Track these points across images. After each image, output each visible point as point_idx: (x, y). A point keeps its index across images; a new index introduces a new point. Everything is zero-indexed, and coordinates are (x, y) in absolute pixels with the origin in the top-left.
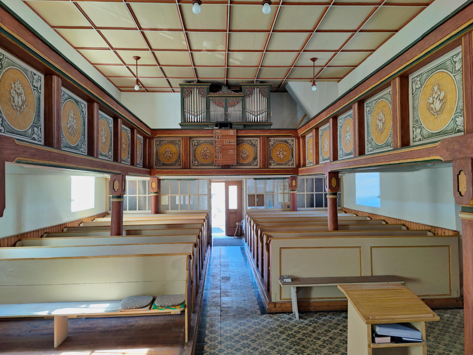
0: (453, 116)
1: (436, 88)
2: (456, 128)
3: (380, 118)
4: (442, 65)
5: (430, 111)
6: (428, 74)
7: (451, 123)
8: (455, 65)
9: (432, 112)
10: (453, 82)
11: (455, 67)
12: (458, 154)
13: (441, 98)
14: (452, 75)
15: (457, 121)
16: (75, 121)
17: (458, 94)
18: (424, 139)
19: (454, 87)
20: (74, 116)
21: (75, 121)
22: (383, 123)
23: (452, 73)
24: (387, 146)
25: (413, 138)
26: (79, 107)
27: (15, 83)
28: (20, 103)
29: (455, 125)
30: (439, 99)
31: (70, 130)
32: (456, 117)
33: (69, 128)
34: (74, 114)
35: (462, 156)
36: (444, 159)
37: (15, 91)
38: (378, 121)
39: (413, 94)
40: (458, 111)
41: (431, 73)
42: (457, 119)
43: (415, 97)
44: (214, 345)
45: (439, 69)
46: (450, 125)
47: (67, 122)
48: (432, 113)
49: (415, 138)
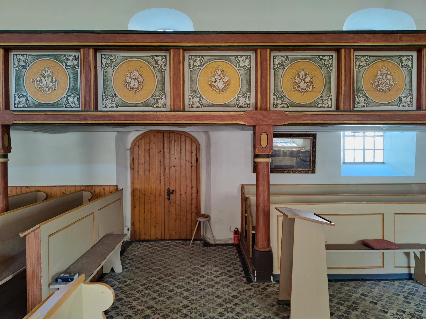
0: (236, 96)
1: (219, 72)
2: (238, 105)
4: (226, 58)
5: (212, 87)
6: (210, 59)
7: (234, 100)
8: (239, 62)
9: (215, 89)
10: (236, 73)
11: (239, 64)
12: (261, 122)
13: (224, 81)
14: (236, 68)
15: (239, 100)
17: (242, 82)
18: (203, 107)
19: (238, 77)
22: (140, 84)
23: (236, 67)
25: (189, 105)
29: (238, 103)
30: (222, 81)
35: (264, 123)
36: (248, 124)
39: (189, 68)
40: (241, 93)
41: (213, 59)
42: (239, 99)
43: (192, 72)
45: (223, 59)
46: (233, 101)
48: (213, 89)
49: (192, 104)
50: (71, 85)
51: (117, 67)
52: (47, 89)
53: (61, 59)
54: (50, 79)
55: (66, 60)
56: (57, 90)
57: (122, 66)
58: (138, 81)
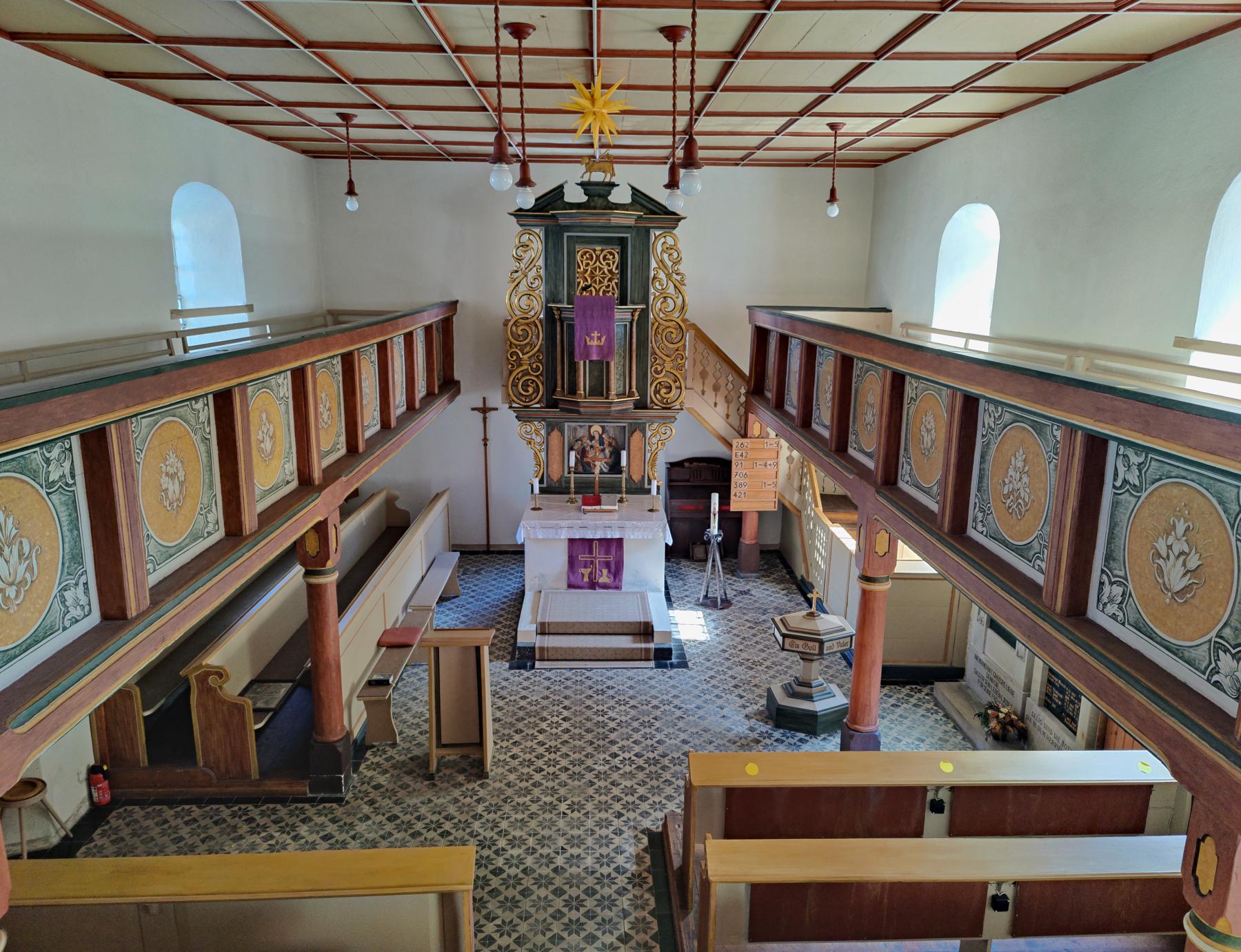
3: (171, 471)
16: (1025, 479)
20: (1024, 466)
21: (1025, 479)
22: (181, 484)
24: (195, 540)
26: (1046, 440)
27: (926, 415)
28: (930, 444)
31: (1009, 501)
32: (285, 463)
33: (1007, 496)
34: (1025, 461)
37: (925, 426)
38: (165, 479)
44: (636, 908)
47: (1004, 482)
50: (67, 546)
51: (144, 452)
52: (11, 592)
53: (34, 466)
54: (15, 549)
55: (45, 466)
56: (36, 582)
57: (151, 445)
58: (178, 478)
